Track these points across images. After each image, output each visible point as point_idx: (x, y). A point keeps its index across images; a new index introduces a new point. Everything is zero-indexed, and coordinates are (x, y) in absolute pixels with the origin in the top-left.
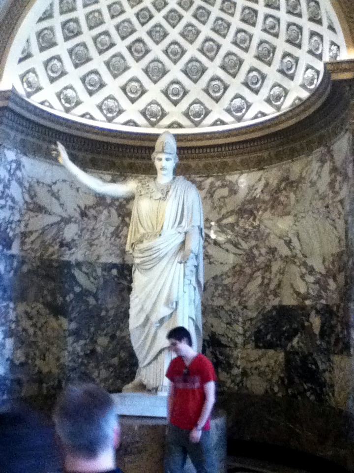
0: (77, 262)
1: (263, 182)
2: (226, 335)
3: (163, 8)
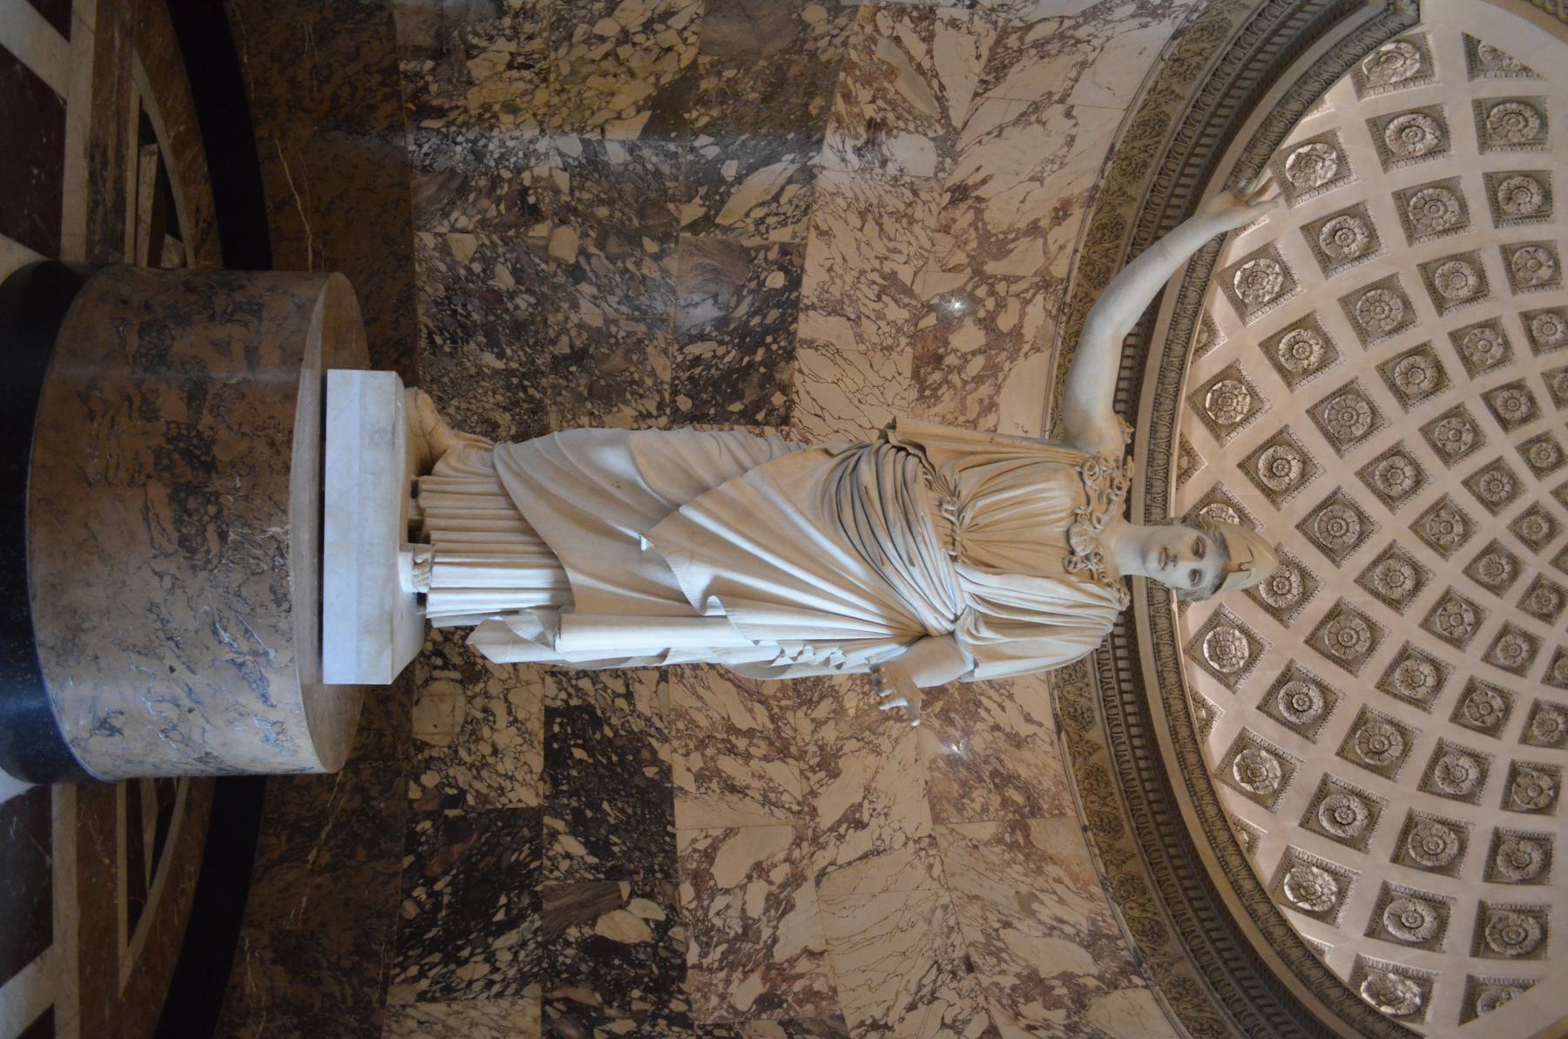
0: (815, 171)
1: (1025, 729)
3: (1528, 461)
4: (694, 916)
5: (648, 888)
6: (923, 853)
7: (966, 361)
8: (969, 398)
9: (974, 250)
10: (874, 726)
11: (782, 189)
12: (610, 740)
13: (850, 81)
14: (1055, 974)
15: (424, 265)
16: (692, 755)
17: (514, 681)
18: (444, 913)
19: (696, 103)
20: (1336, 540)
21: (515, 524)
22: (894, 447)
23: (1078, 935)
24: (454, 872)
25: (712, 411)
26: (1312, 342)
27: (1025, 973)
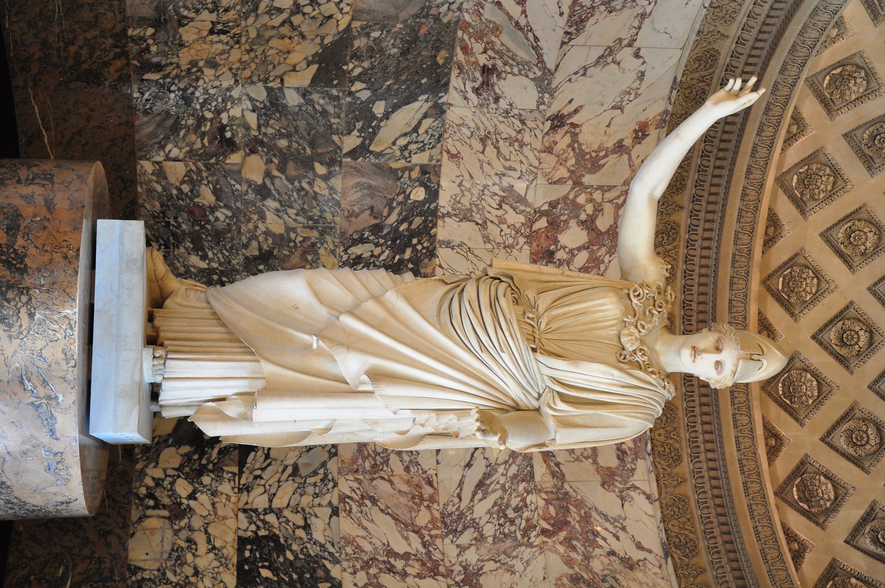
0: (444, 107)
1: (637, 555)
2: (269, 465)
7: (574, 256)
9: (573, 166)
10: (509, 551)
11: (420, 123)
12: (291, 562)
13: (466, 37)
15: (144, 187)
16: (358, 573)
17: (212, 517)
19: (352, 58)
22: (491, 278)
26: (866, 230)
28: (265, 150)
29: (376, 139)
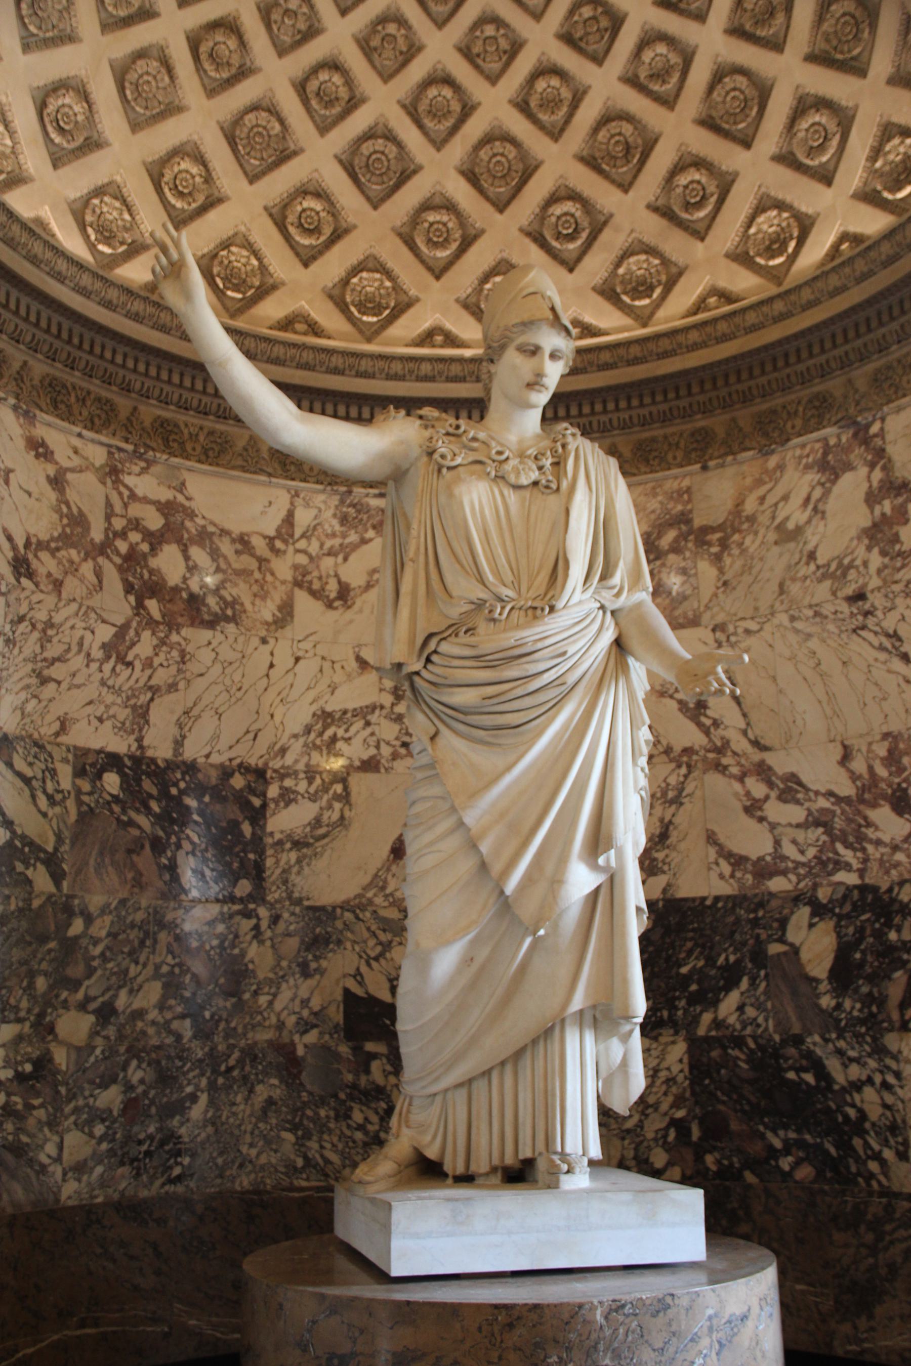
4: (805, 876)
5: (775, 925)
6: (733, 639)
8: (236, 566)
9: (79, 553)
11: (19, 774)
14: (867, 511)
15: (96, 1192)
18: (808, 1137)
20: (393, 168)
21: (509, 1069)
22: (425, 667)
23: (823, 485)
24: (761, 1128)
25: (251, 856)
26: (176, 169)
27: (866, 541)
28: (49, 1010)
29: (38, 841)
